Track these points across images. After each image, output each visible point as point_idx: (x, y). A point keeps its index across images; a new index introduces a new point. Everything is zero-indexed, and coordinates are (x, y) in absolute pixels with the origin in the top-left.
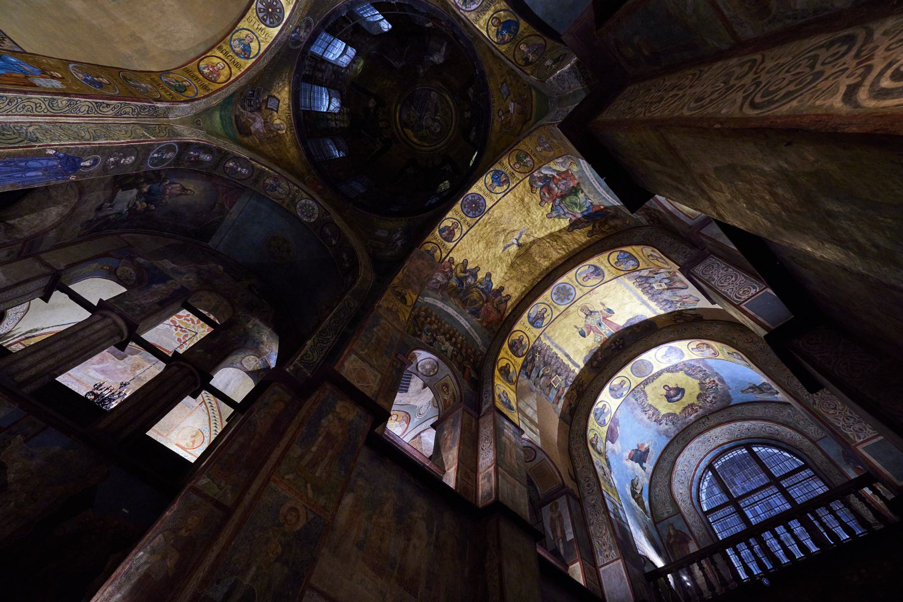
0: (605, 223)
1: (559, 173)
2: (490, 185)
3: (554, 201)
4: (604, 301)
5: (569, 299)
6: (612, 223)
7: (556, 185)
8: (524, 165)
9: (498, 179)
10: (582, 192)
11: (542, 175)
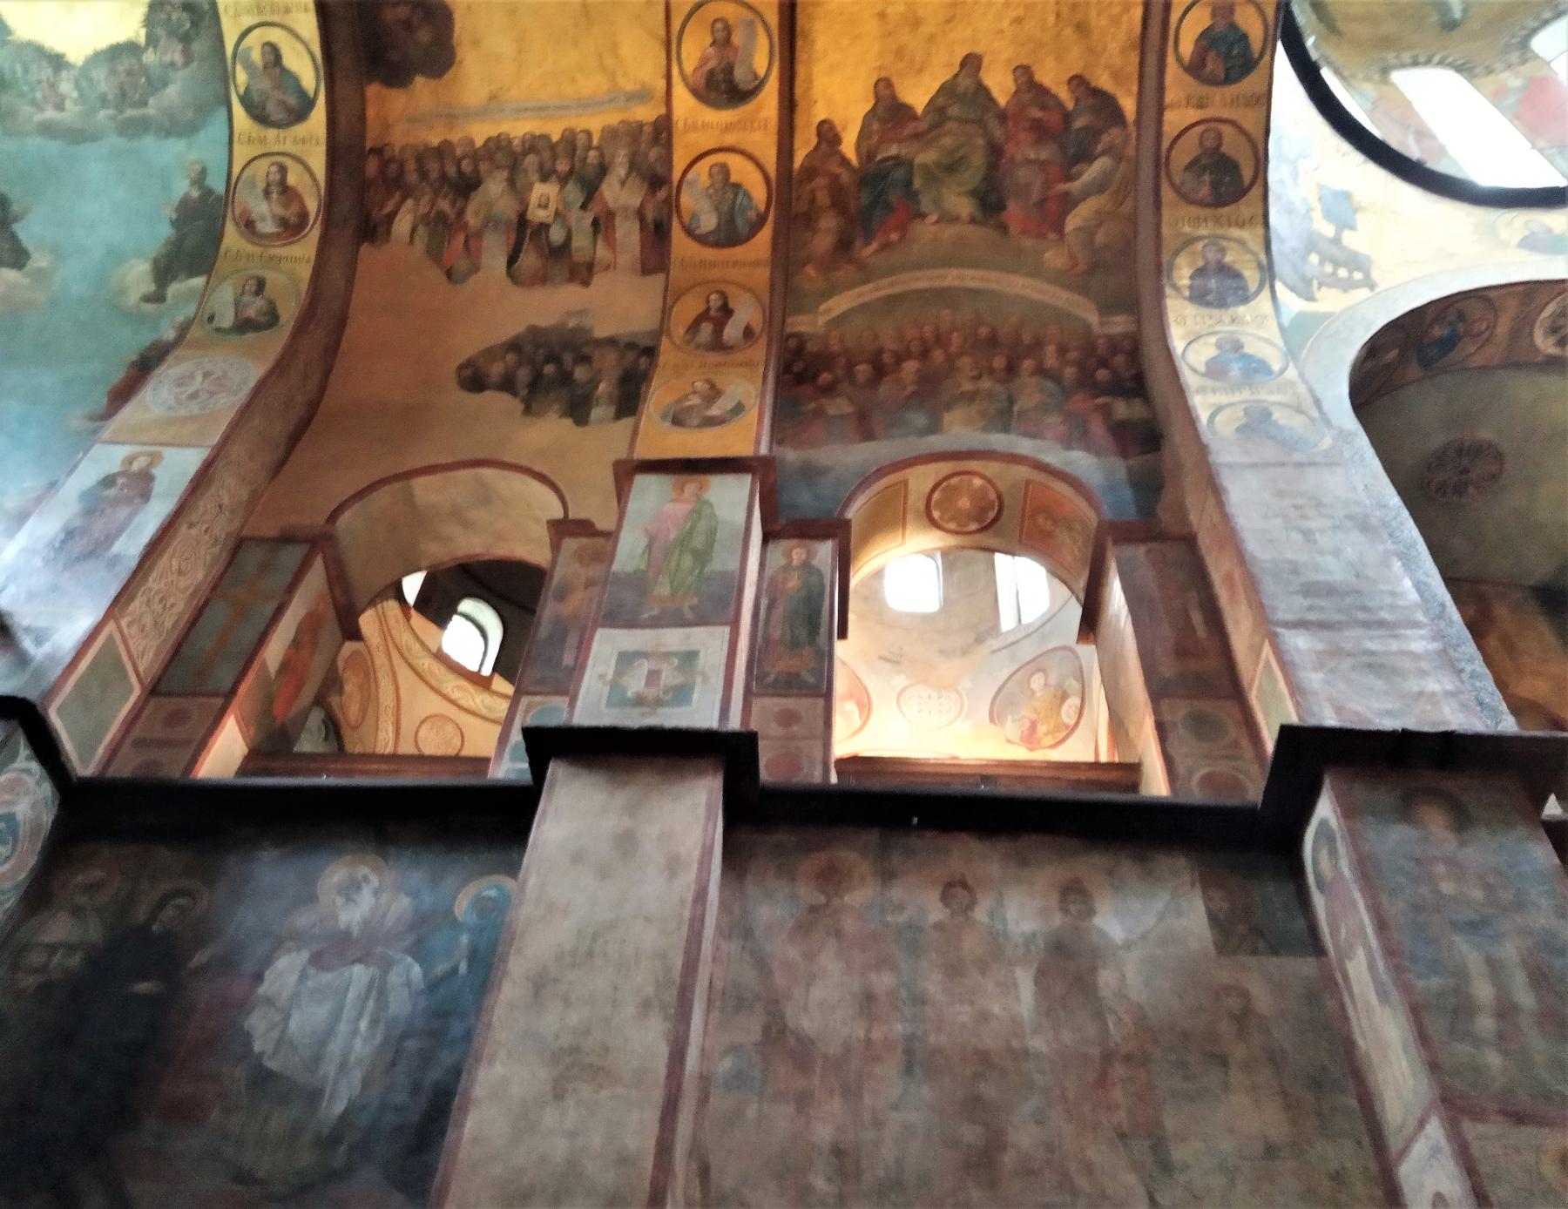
0: (839, 205)
1: (1068, 203)
3: (1003, 116)
6: (828, 223)
7: (1042, 165)
10: (973, 221)
11: (1100, 148)
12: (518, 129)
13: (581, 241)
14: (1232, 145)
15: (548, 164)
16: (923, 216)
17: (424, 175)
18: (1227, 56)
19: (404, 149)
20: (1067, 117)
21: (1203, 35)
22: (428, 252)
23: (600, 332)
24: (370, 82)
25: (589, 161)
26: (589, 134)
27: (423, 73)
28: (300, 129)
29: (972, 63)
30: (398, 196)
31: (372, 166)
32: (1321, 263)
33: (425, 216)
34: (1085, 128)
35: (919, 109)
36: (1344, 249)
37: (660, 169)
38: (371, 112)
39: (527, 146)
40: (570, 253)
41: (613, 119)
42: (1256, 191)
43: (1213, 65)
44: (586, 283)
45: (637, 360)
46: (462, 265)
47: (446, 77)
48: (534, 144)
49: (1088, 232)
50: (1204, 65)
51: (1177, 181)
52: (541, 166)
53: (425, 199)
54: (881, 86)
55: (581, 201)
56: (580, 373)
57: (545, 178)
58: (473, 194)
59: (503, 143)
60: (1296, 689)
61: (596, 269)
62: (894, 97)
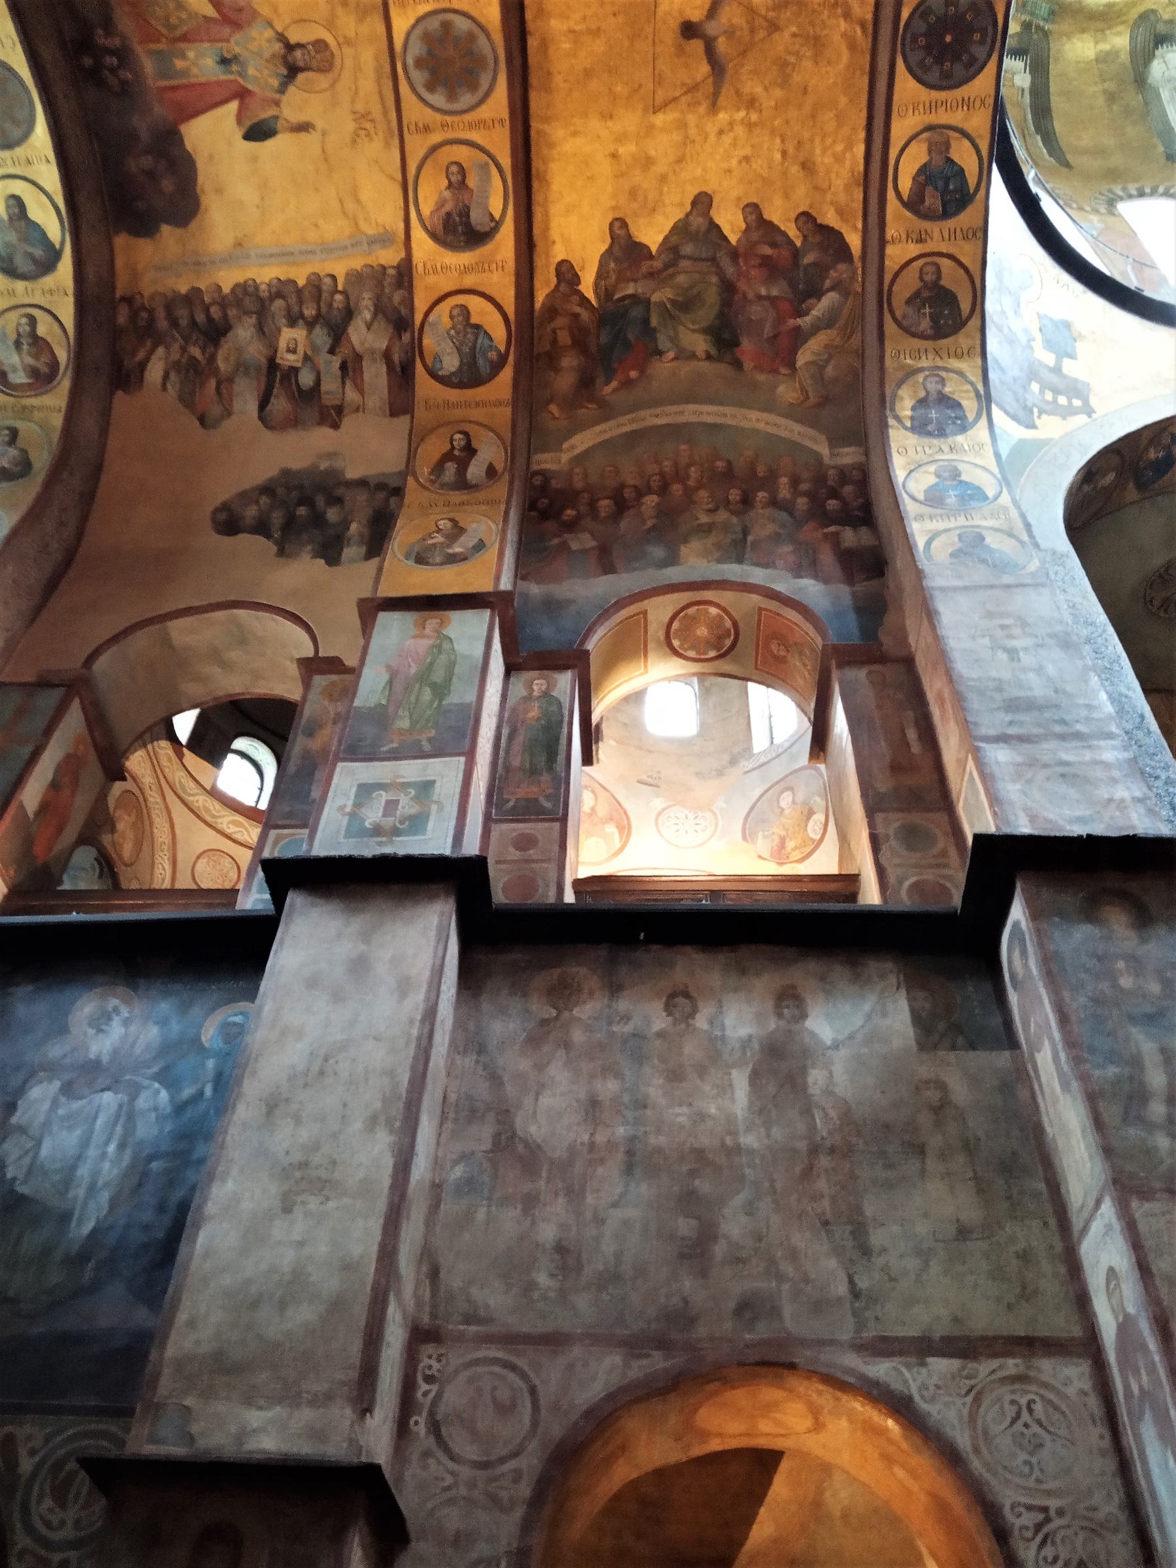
0: (580, 343)
1: (799, 337)
2: (948, 146)
3: (734, 254)
4: (310, 140)
5: (419, 63)
6: (569, 362)
7: (772, 300)
8: (917, 294)
9: (940, 184)
10: (709, 357)
12: (266, 275)
13: (330, 385)
14: (950, 277)
15: (296, 309)
16: (660, 353)
17: (174, 323)
18: (945, 191)
19: (152, 297)
20: (796, 253)
21: (923, 170)
22: (181, 399)
23: (352, 474)
24: (117, 232)
25: (335, 305)
26: (333, 278)
27: (168, 223)
28: (48, 281)
29: (703, 202)
30: (149, 343)
31: (122, 316)
32: (1042, 392)
33: (177, 365)
34: (814, 264)
35: (654, 249)
36: (1065, 376)
37: (404, 311)
38: (119, 262)
39: (274, 290)
40: (320, 397)
41: (357, 263)
42: (974, 323)
43: (932, 200)
44: (336, 426)
45: (387, 500)
46: (216, 410)
47: (194, 225)
48: (282, 289)
49: (818, 367)
50: (922, 201)
51: (898, 314)
52: (289, 309)
53: (176, 347)
54: (617, 224)
55: (328, 346)
56: (332, 514)
57: (292, 323)
58: (223, 340)
59: (251, 289)
60: (994, 800)
61: (346, 411)
62: (629, 236)
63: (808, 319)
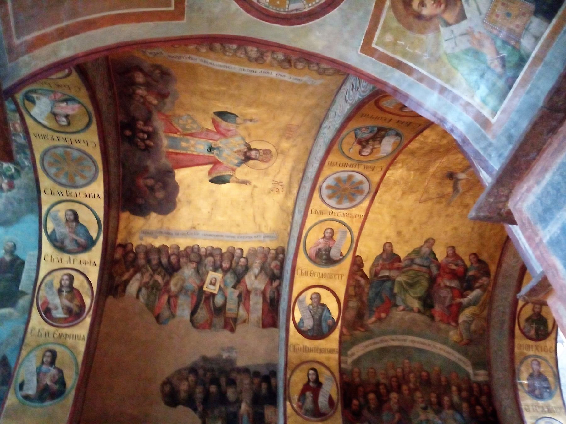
1: (461, 308)
3: (439, 266)
4: (246, 189)
7: (452, 288)
10: (419, 311)
11: (477, 285)
12: (204, 244)
13: (231, 305)
15: (218, 263)
16: (397, 306)
17: (148, 261)
19: (138, 247)
20: (466, 270)
22: (147, 305)
23: (241, 363)
24: (124, 210)
25: (240, 263)
26: (242, 250)
27: (155, 211)
28: (84, 256)
29: (430, 242)
30: (132, 270)
31: (118, 255)
33: (146, 285)
34: (473, 276)
35: (402, 259)
37: (276, 272)
38: (122, 225)
39: (208, 252)
40: (225, 313)
41: (256, 245)
44: (232, 330)
45: (260, 386)
46: (166, 313)
47: (169, 216)
48: (211, 253)
49: (468, 323)
51: (522, 326)
52: (215, 262)
53: (147, 275)
54: (388, 245)
55: (233, 284)
56: (231, 394)
57: (215, 270)
58: (175, 274)
59: (196, 250)
61: (239, 322)
62: (392, 250)
63: (466, 299)
